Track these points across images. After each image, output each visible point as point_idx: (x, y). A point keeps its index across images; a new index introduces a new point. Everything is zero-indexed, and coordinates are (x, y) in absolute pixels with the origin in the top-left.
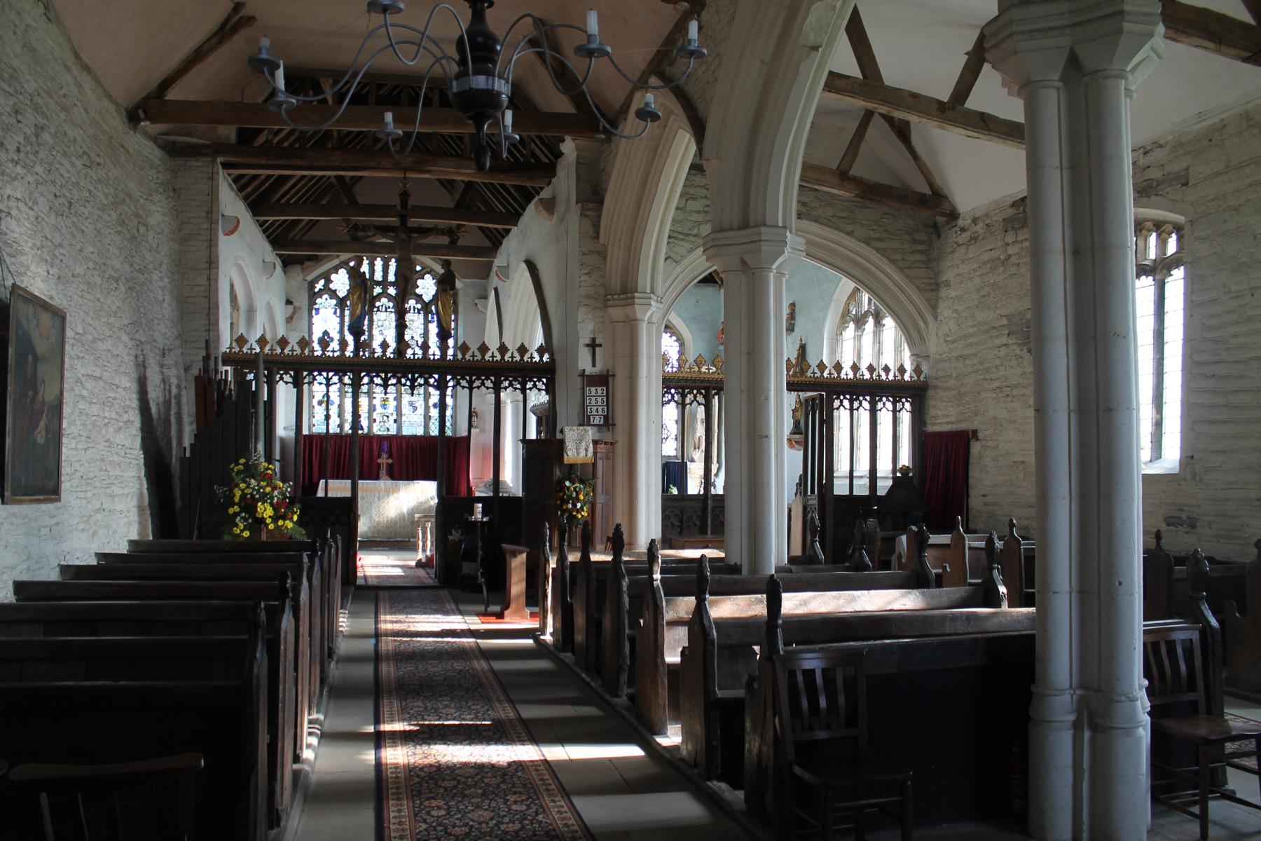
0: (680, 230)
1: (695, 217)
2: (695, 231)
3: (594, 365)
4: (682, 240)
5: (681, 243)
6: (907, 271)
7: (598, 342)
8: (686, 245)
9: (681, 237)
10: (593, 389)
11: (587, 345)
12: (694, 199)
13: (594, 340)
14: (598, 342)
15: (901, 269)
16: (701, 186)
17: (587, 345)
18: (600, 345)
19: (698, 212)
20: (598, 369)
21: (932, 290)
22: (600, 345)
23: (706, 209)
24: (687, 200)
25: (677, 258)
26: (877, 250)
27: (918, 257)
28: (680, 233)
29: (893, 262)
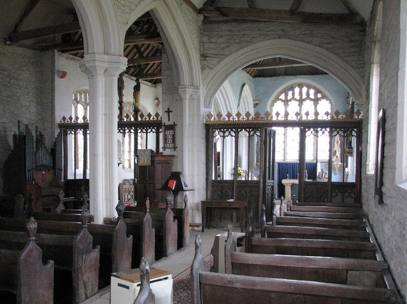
0: (214, 53)
1: (222, 45)
2: (222, 52)
3: (169, 120)
4: (214, 57)
5: (214, 59)
6: (346, 59)
7: (170, 110)
8: (217, 60)
9: (214, 56)
10: (168, 131)
11: (166, 112)
12: (221, 37)
13: (169, 109)
14: (170, 110)
15: (341, 58)
16: (225, 30)
17: (166, 112)
18: (171, 111)
19: (223, 43)
20: (171, 123)
21: (362, 67)
22: (171, 111)
23: (228, 41)
24: (218, 38)
25: (211, 67)
26: (327, 49)
27: (353, 50)
28: (214, 54)
29: (337, 54)
